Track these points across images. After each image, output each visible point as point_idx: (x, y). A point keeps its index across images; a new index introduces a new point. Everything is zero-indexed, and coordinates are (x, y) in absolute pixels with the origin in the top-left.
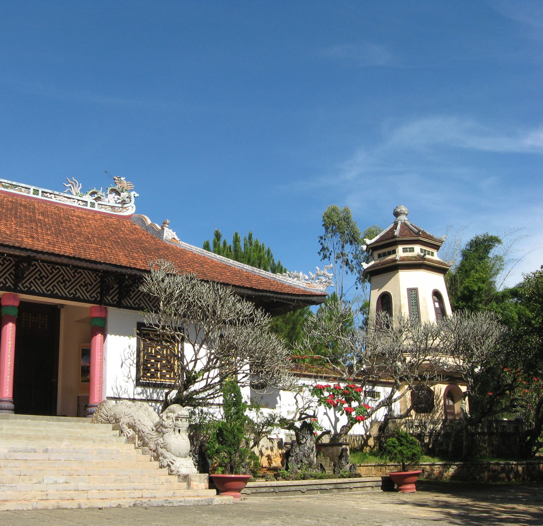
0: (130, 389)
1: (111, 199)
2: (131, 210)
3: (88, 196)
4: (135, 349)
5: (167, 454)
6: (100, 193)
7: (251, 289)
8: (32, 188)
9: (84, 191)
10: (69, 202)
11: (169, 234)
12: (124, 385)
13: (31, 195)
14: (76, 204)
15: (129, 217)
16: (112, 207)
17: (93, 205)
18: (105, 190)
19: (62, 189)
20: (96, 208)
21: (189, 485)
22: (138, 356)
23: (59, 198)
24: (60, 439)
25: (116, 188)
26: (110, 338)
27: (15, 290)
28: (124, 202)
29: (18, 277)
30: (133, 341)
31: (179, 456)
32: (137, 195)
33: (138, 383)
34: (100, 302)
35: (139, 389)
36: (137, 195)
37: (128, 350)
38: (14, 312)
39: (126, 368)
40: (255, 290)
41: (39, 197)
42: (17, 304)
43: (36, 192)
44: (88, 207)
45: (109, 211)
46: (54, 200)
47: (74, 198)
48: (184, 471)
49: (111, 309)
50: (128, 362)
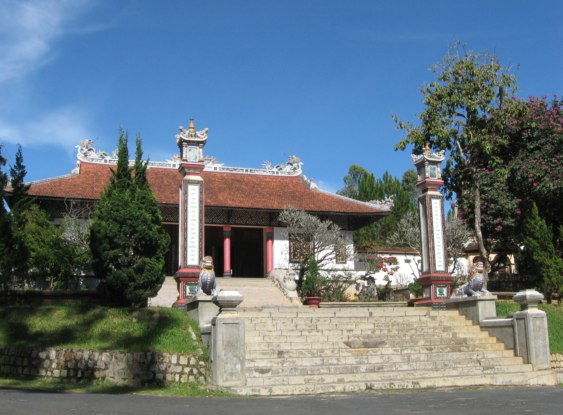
0: (287, 265)
1: (288, 168)
2: (299, 172)
3: (275, 168)
4: (288, 246)
5: (286, 290)
6: (281, 166)
7: (344, 212)
8: (245, 169)
9: (272, 167)
10: (265, 174)
11: (313, 185)
12: (283, 263)
13: (244, 173)
14: (268, 174)
15: (298, 176)
16: (289, 173)
17: (277, 173)
18: (284, 164)
19: (260, 167)
20: (280, 175)
21: (292, 301)
22: (290, 249)
23: (259, 172)
24: (244, 286)
25: (291, 162)
26: (276, 242)
27: (228, 224)
28: (295, 169)
29: (229, 218)
30: (287, 242)
31: (291, 290)
32: (302, 164)
33: (290, 261)
34: (269, 226)
35: (291, 265)
36: (302, 164)
37: (285, 246)
38: (229, 234)
39: (284, 255)
40: (346, 213)
41: (249, 173)
42: (230, 229)
43: (247, 171)
44: (275, 175)
45: (287, 175)
46: (256, 173)
47: (268, 171)
48: (291, 296)
49: (275, 228)
50: (284, 252)
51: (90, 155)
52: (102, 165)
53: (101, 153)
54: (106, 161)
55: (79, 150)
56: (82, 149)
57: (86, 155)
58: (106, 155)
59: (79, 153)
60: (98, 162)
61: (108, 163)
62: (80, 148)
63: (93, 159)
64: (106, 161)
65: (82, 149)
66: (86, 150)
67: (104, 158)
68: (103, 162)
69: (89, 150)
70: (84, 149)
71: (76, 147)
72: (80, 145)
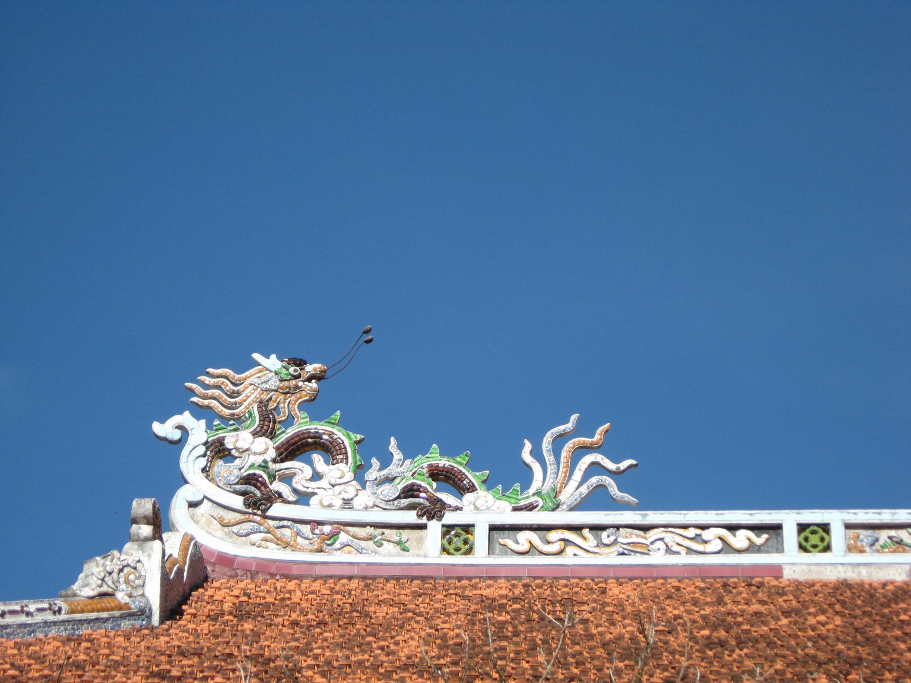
51: (303, 498)
52: (424, 579)
53: (407, 469)
54: (458, 536)
55: (191, 462)
56: (218, 451)
57: (257, 495)
58: (460, 487)
59: (197, 484)
60: (387, 554)
61: (480, 556)
62: (199, 432)
63: (329, 533)
64: (458, 536)
65: (218, 451)
66: (255, 449)
67: (435, 510)
68: (428, 550)
69: (294, 449)
70: (240, 439)
71: (165, 429)
72: (200, 412)
